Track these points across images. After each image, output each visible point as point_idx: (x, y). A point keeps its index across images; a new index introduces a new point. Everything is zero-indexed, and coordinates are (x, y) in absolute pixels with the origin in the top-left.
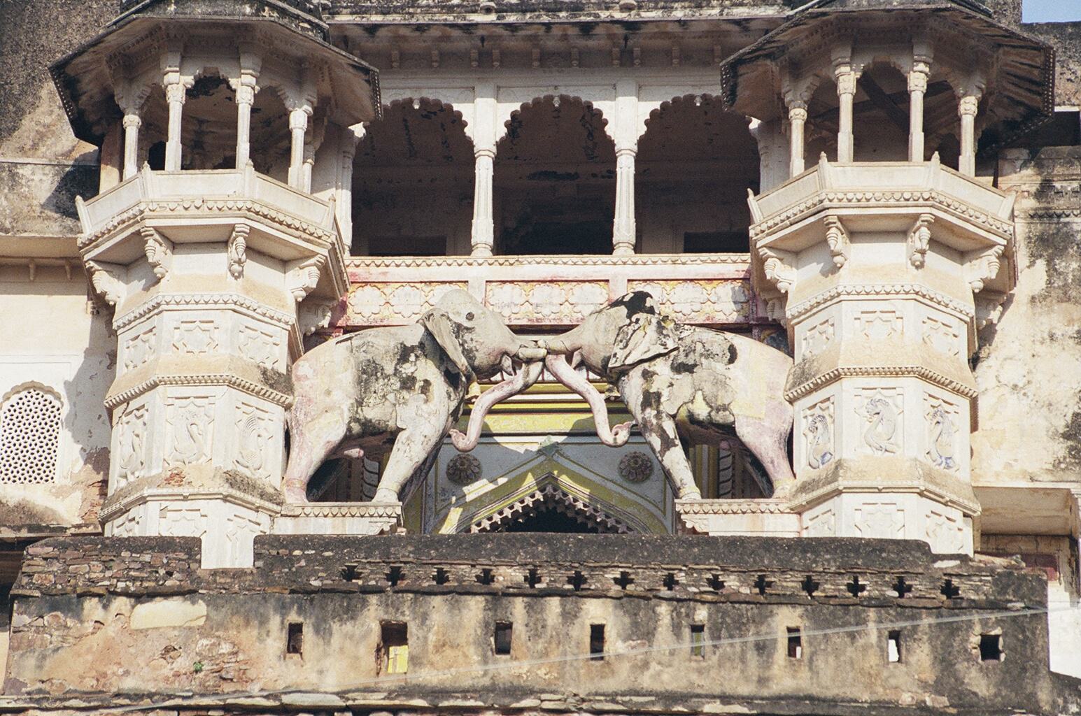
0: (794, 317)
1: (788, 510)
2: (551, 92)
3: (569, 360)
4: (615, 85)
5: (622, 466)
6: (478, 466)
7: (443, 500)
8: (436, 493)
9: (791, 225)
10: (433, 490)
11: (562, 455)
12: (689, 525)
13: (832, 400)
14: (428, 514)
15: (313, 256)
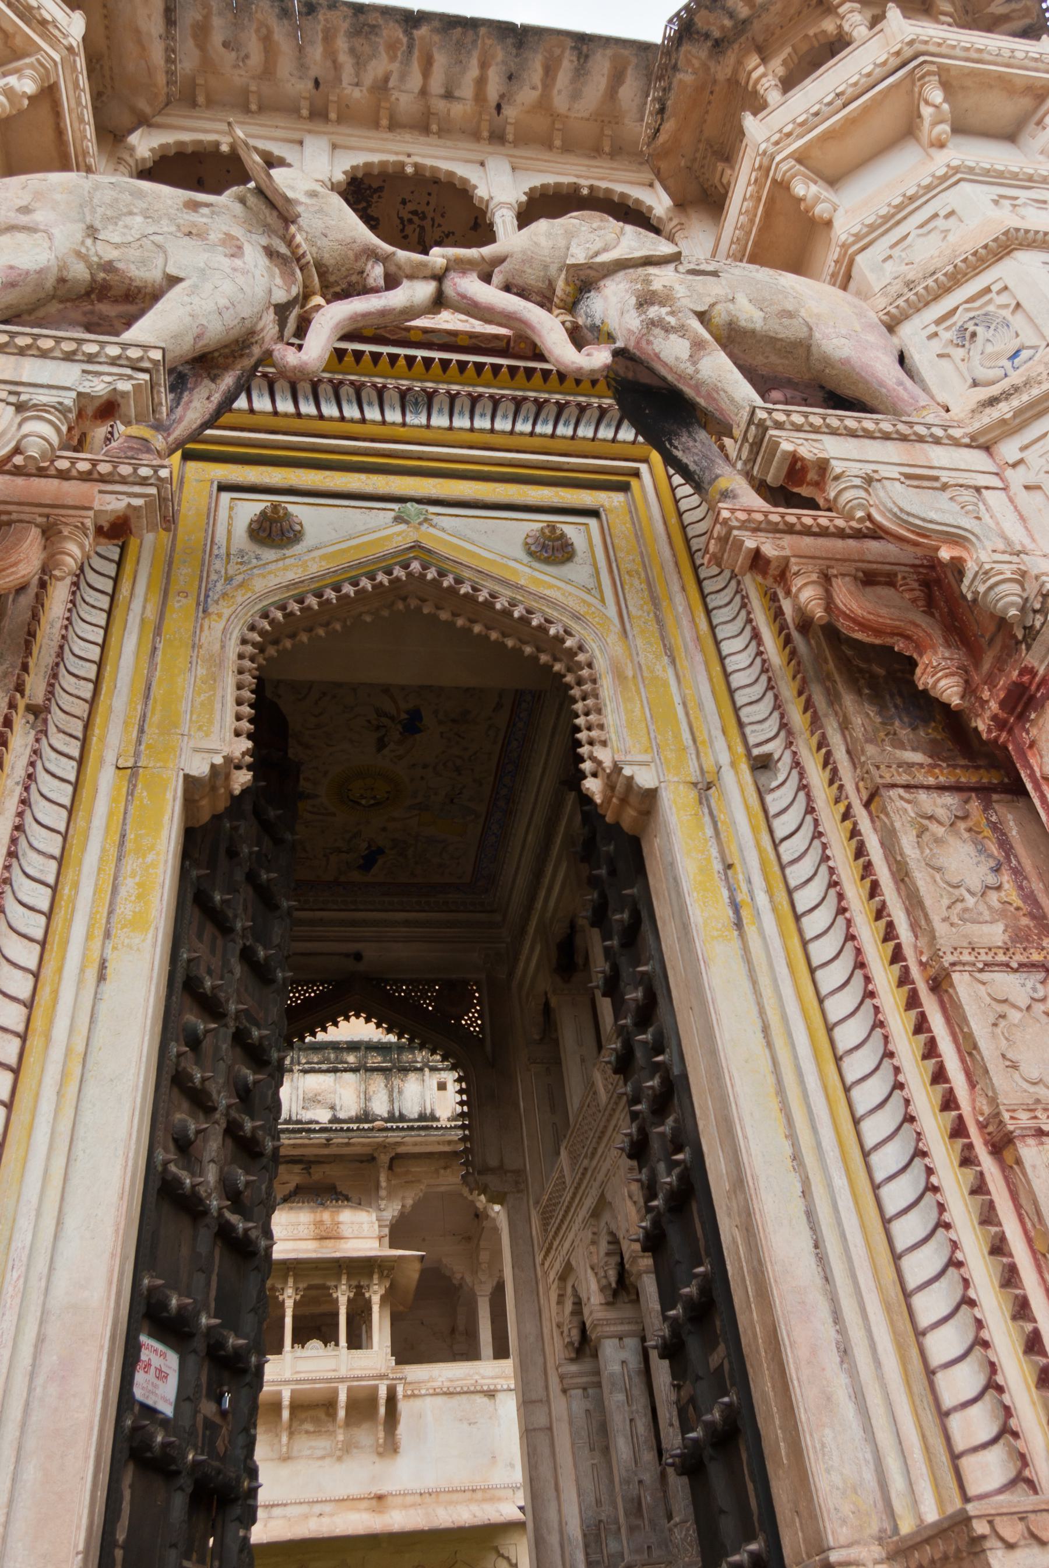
0: (858, 237)
1: (967, 440)
2: (402, 158)
3: (487, 278)
4: (482, 164)
5: (530, 541)
6: (301, 524)
7: (241, 563)
8: (228, 555)
9: (845, 106)
10: (223, 551)
11: (434, 527)
12: (786, 446)
13: (995, 288)
14: (214, 577)
15: (28, 55)
